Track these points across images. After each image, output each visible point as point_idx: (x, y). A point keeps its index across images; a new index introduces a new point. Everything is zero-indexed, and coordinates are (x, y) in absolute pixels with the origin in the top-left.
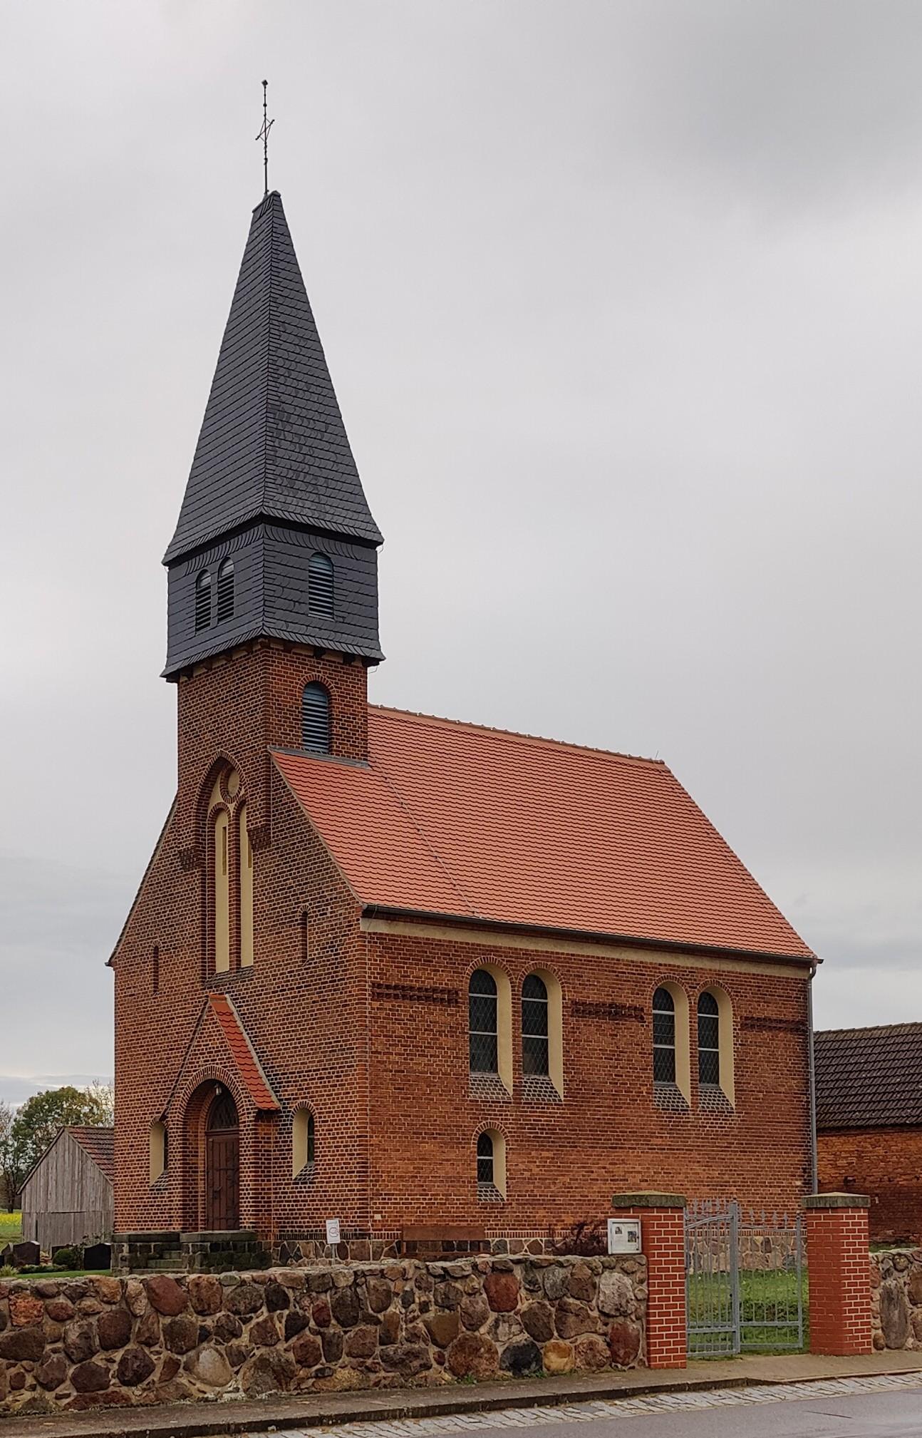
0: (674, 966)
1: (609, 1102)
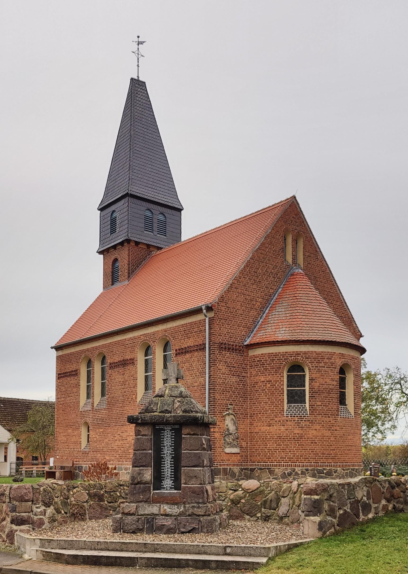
0: (147, 334)
1: (121, 405)
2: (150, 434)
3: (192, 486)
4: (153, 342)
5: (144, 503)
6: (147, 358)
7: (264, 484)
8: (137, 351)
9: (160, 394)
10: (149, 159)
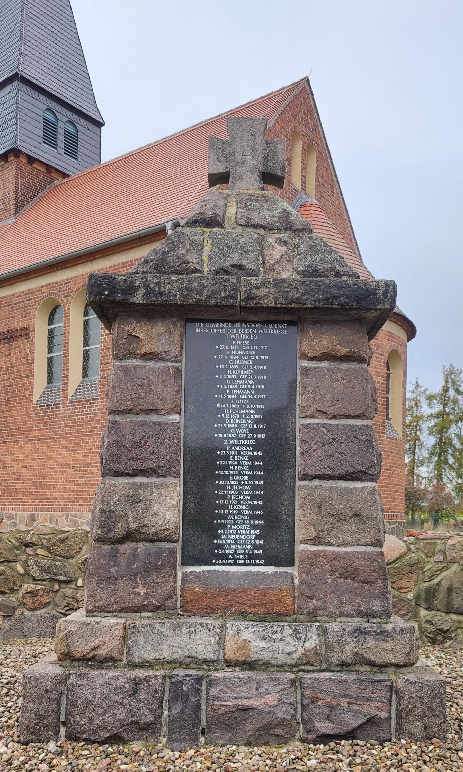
0: (53, 283)
2: (175, 351)
3: (342, 549)
4: (65, 297)
5: (149, 614)
6: (51, 327)
7: (417, 546)
8: (35, 315)
9: (209, 214)
10: (53, 34)
